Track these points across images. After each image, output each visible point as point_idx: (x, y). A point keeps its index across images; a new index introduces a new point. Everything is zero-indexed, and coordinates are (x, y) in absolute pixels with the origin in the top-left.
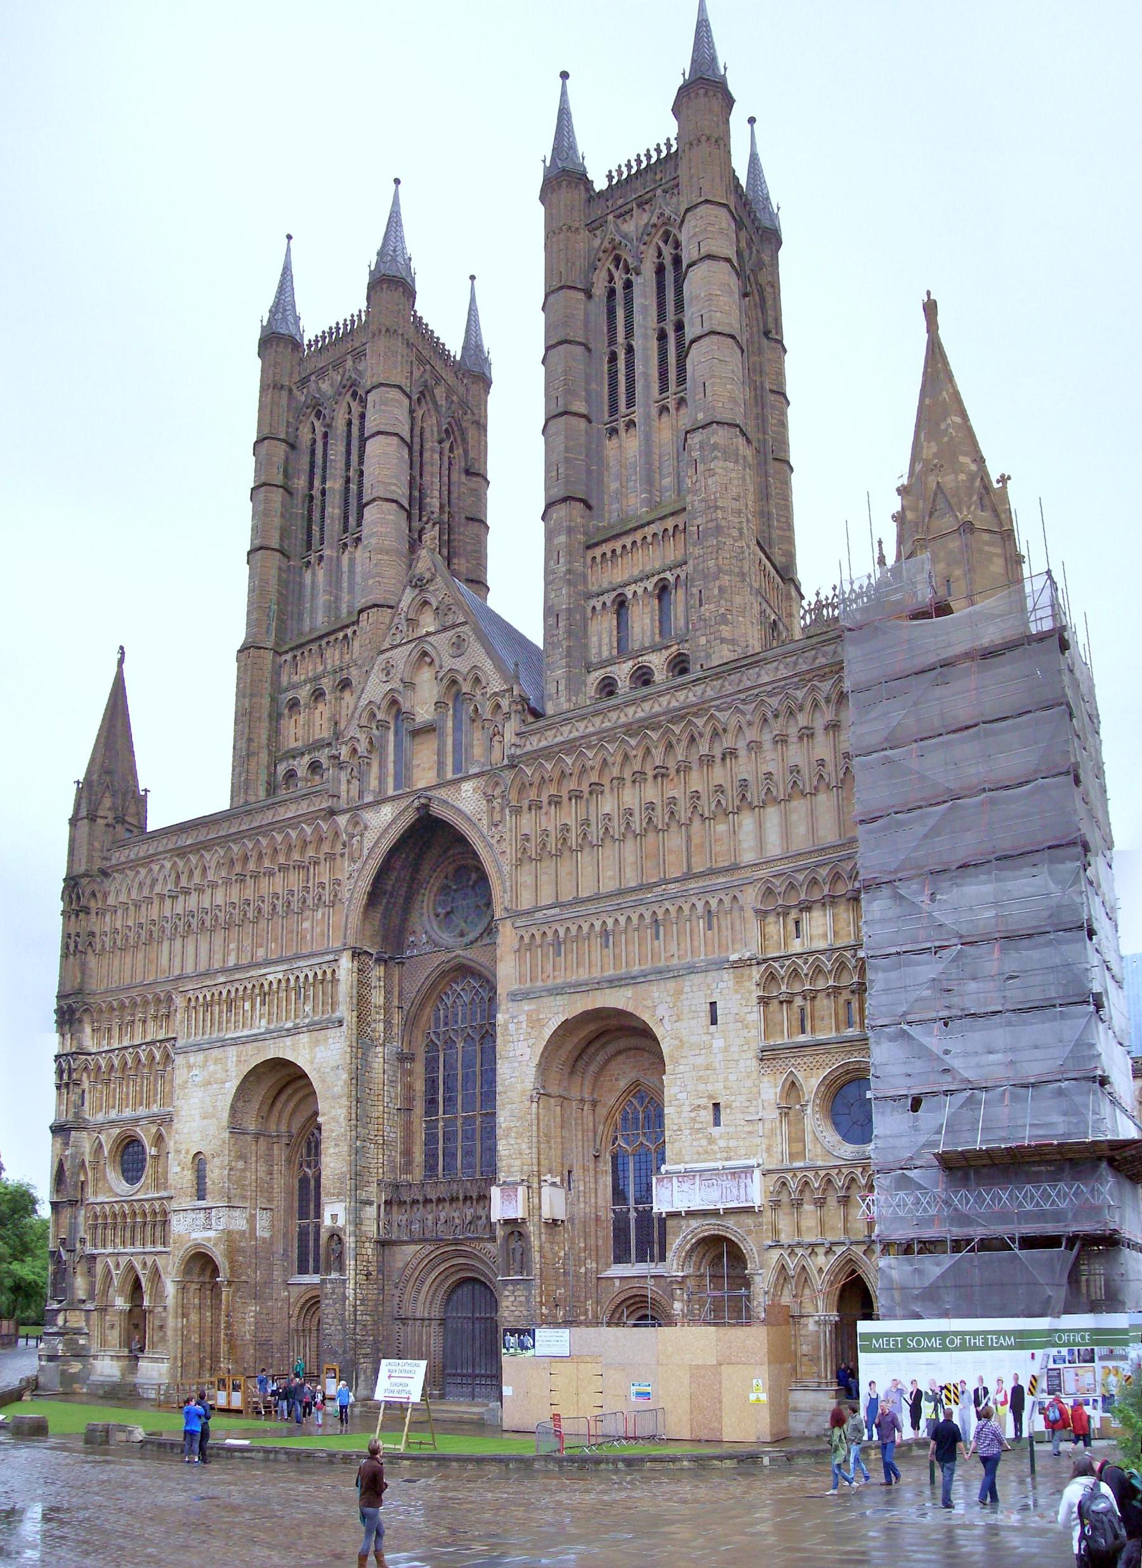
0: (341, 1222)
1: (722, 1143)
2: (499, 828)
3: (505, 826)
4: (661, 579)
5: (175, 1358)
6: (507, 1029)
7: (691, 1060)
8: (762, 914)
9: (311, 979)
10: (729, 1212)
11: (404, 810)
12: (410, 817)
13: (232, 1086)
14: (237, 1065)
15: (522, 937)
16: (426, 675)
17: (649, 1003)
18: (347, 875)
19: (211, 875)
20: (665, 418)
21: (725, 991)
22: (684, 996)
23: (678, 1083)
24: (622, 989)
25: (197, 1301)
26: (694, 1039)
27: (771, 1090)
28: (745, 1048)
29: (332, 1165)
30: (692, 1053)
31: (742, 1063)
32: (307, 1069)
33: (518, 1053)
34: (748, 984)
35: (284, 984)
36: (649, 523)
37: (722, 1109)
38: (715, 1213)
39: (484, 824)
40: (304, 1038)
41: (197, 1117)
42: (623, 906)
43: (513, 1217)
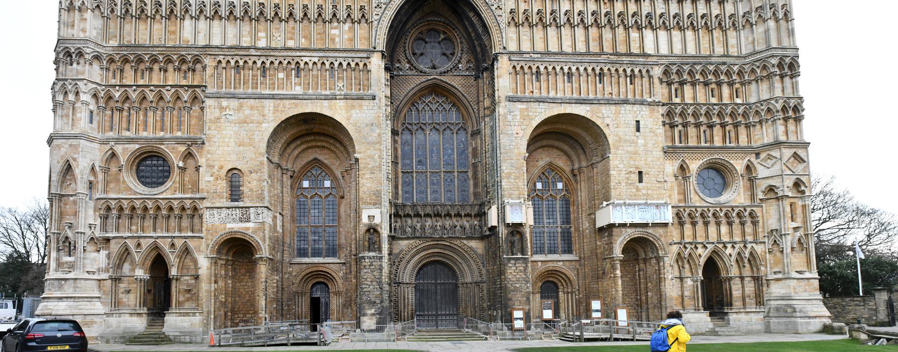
0: (377, 221)
1: (644, 192)
5: (209, 313)
6: (506, 118)
7: (626, 148)
8: (661, 81)
9: (345, 66)
10: (655, 225)
13: (269, 127)
14: (274, 113)
15: (514, 67)
17: (600, 115)
18: (374, 5)
21: (644, 116)
22: (621, 115)
23: (618, 159)
25: (223, 272)
26: (627, 138)
27: (671, 167)
28: (656, 145)
29: (368, 185)
30: (626, 145)
31: (654, 153)
32: (344, 123)
33: (514, 132)
34: (656, 114)
35: (319, 65)
37: (644, 175)
38: (646, 225)
40: (342, 103)
41: (232, 144)
43: (519, 222)
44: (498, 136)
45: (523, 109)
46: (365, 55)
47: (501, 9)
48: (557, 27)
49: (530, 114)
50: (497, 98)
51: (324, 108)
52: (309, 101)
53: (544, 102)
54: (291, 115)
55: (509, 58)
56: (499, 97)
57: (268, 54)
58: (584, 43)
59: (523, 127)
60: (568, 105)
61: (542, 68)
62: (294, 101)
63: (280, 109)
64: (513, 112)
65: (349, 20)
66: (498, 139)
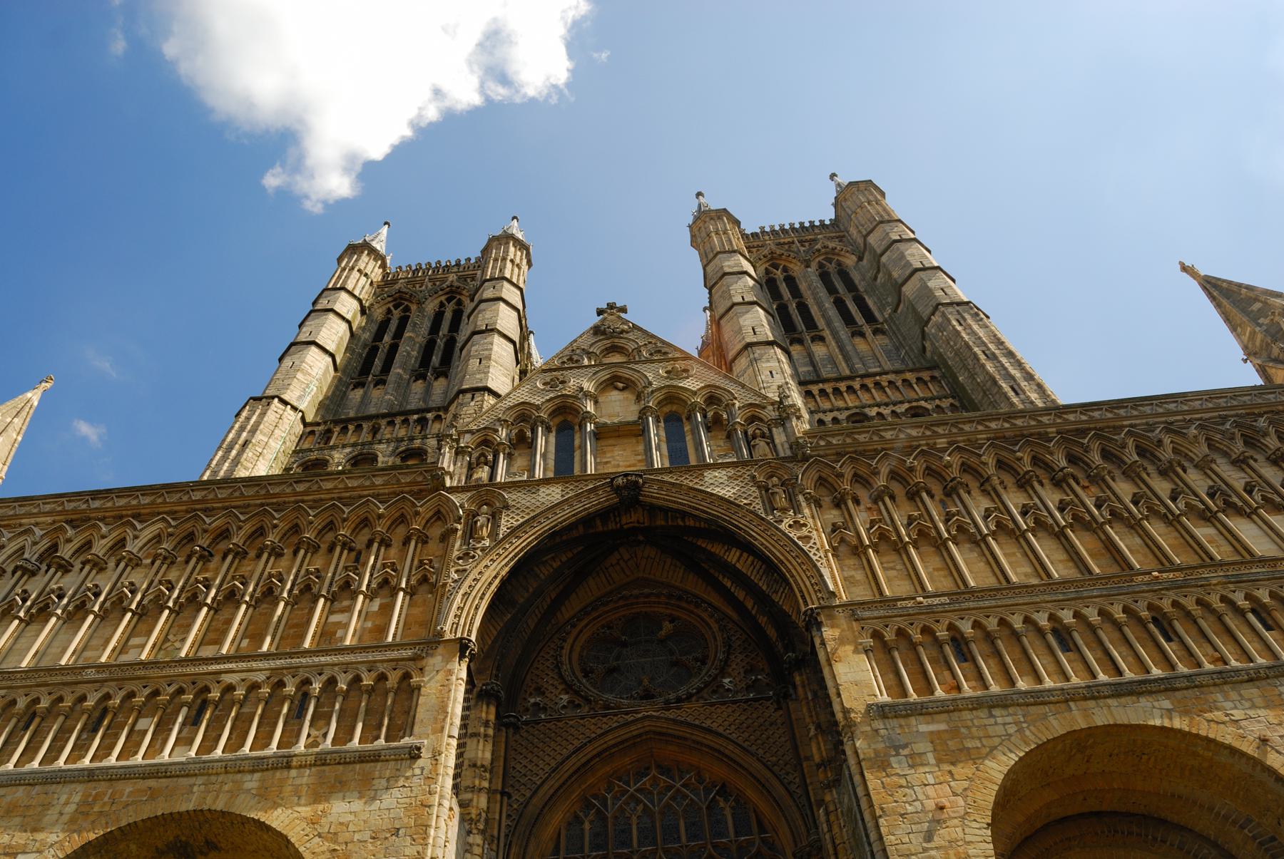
2: (791, 513)
3: (798, 510)
4: (911, 408)
11: (590, 491)
12: (602, 499)
16: (615, 396)
19: (133, 547)
20: (858, 340)
24: (1143, 700)
35: (265, 690)
36: (880, 374)
39: (758, 507)
40: (306, 778)
42: (1085, 594)
44: (870, 825)
45: (939, 732)
46: (409, 653)
47: (805, 525)
48: (976, 543)
49: (969, 744)
50: (839, 716)
51: (243, 796)
52: (200, 780)
53: (1005, 707)
54: (123, 823)
55: (853, 615)
56: (846, 712)
57: (128, 674)
58: (1071, 564)
59: (959, 786)
60: (1091, 703)
61: (966, 628)
62: (152, 783)
63: (96, 809)
64: (905, 746)
65: (385, 591)
66: (873, 836)
